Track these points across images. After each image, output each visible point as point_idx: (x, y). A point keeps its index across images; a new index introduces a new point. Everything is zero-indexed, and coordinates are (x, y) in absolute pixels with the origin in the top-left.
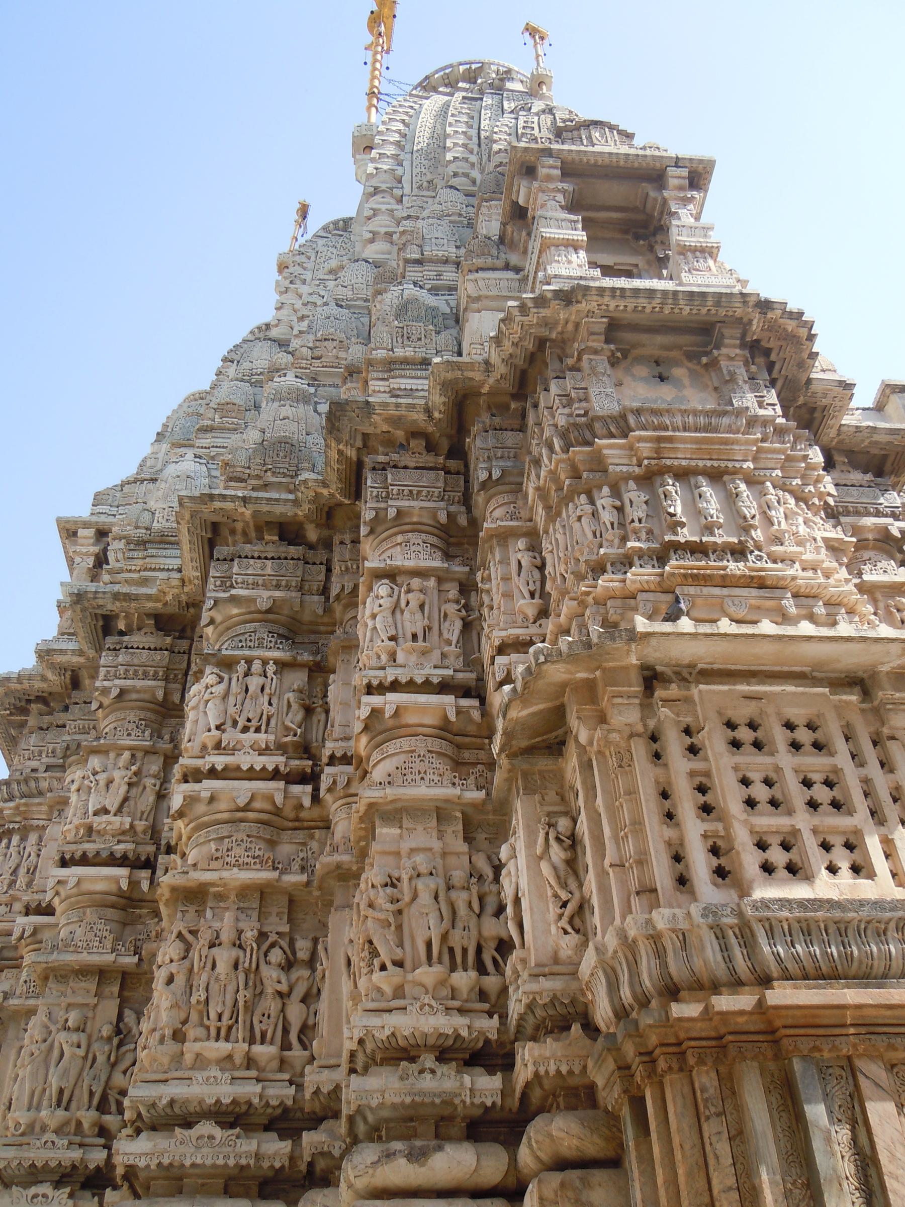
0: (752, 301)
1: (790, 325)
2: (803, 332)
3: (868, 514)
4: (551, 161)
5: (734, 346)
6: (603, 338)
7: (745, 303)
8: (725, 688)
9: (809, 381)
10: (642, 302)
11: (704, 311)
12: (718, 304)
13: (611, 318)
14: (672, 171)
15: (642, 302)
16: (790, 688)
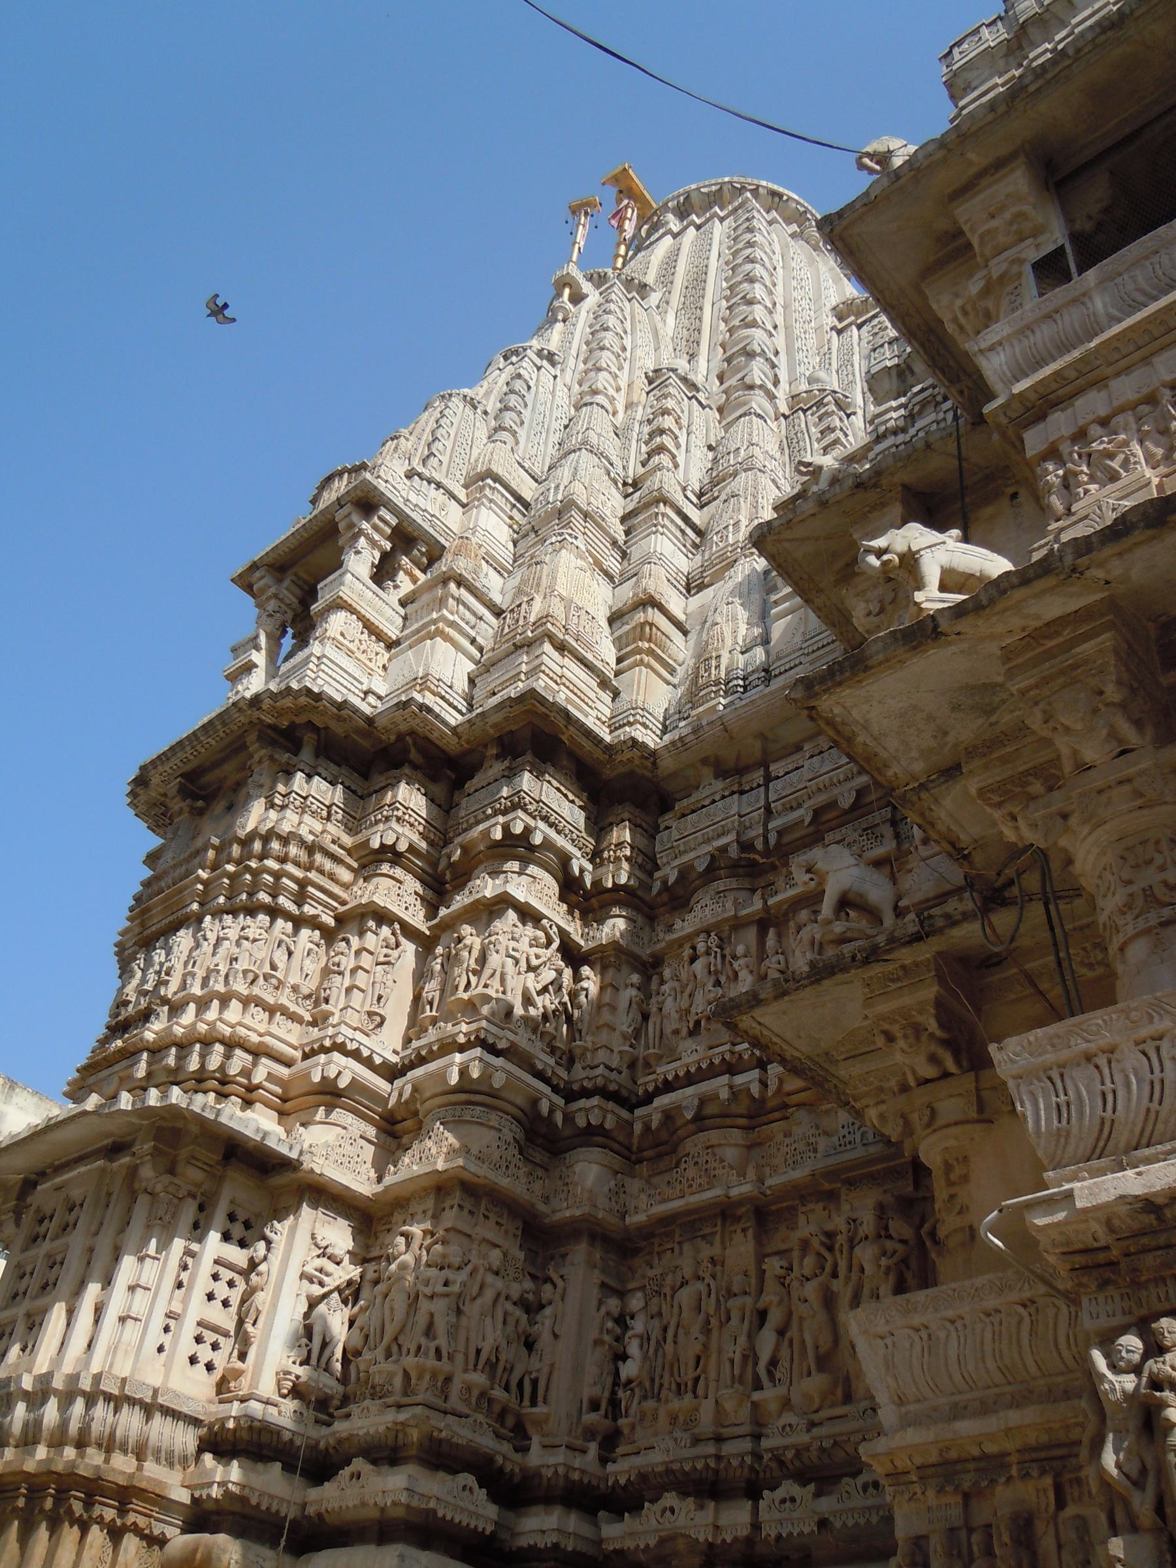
0: (241, 704)
1: (288, 702)
2: (303, 700)
3: (470, 827)
4: (258, 574)
5: (257, 751)
6: (178, 799)
7: (240, 710)
8: (48, 1184)
9: (370, 721)
10: (181, 755)
11: (221, 734)
12: (224, 724)
13: (181, 775)
14: (338, 516)
15: (181, 755)
16: (82, 1169)
